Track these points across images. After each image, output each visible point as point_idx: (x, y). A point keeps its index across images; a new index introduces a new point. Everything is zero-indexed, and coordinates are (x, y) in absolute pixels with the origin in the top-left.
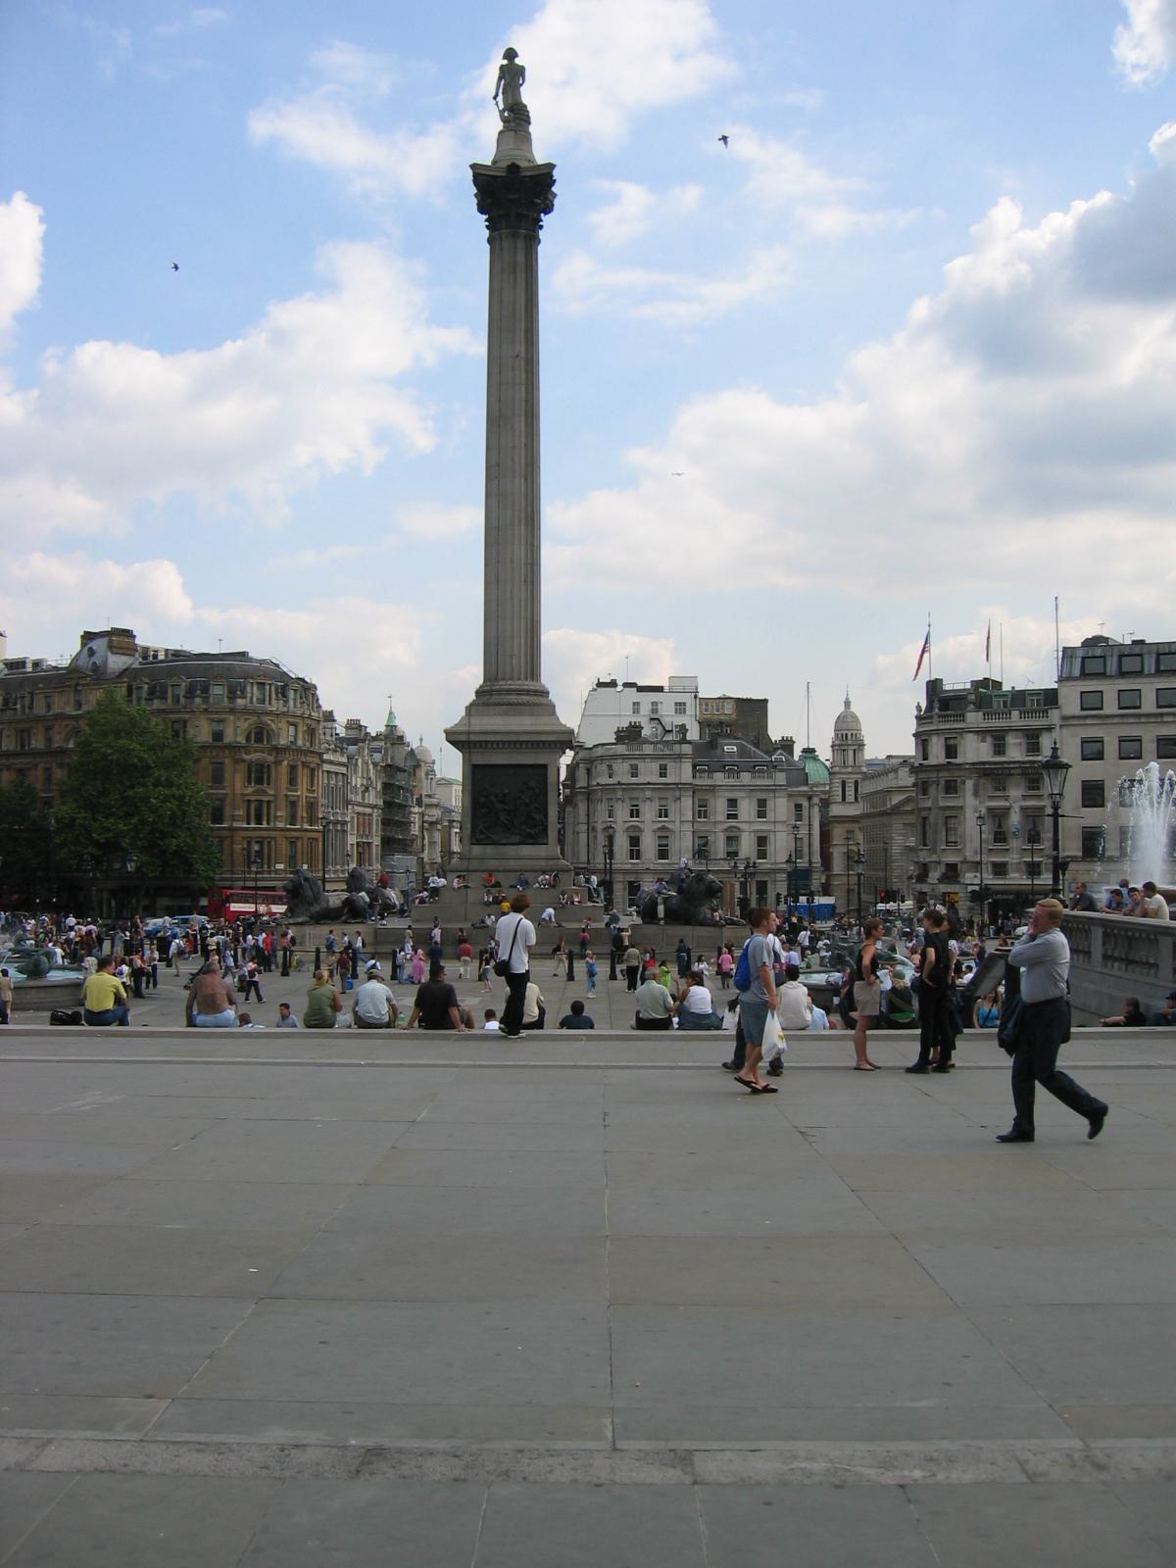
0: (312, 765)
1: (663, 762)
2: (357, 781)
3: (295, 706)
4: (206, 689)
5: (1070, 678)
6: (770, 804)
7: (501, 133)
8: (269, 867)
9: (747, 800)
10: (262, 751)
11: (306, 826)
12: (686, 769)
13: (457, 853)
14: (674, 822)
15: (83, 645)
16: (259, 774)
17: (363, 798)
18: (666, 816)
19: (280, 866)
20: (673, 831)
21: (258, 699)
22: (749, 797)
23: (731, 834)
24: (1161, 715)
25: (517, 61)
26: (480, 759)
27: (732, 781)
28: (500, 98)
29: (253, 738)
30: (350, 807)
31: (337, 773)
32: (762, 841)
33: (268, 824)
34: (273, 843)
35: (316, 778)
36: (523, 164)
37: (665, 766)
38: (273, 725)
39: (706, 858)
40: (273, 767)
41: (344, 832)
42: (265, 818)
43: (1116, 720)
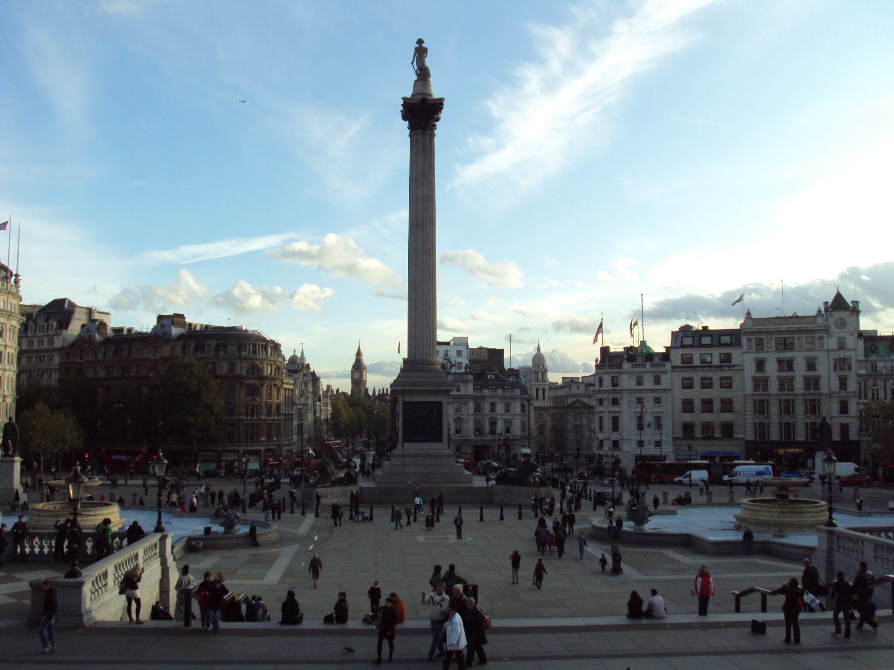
0: (279, 386)
3: (271, 355)
4: (225, 347)
5: (675, 348)
6: (512, 405)
7: (416, 82)
8: (257, 439)
9: (500, 404)
11: (276, 417)
15: (158, 322)
16: (254, 391)
19: (263, 439)
20: (463, 420)
24: (722, 367)
25: (424, 45)
26: (408, 399)
27: (492, 394)
28: (415, 63)
32: (508, 423)
33: (257, 417)
34: (260, 427)
36: (427, 97)
39: (482, 434)
40: (260, 388)
41: (292, 419)
42: (256, 414)
43: (699, 369)
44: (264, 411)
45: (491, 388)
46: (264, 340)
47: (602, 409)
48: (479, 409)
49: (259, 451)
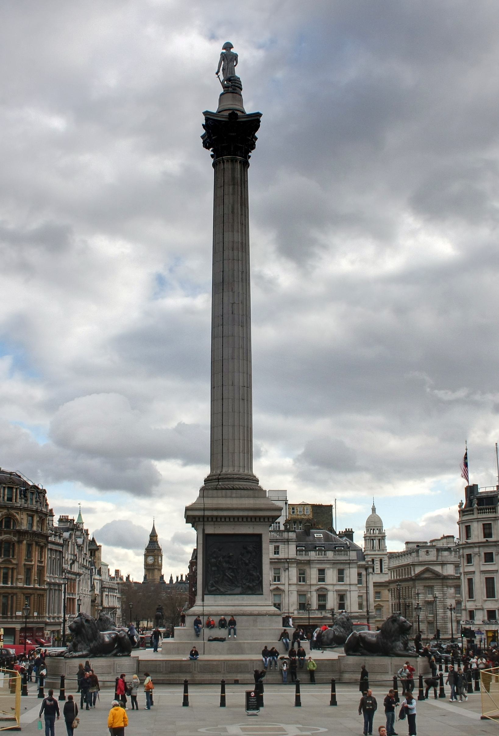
0: (42, 544)
1: (277, 544)
2: (68, 556)
6: (346, 572)
8: (12, 614)
9: (331, 570)
10: (9, 533)
11: (37, 586)
12: (292, 548)
13: (106, 608)
14: (284, 584)
17: (71, 568)
18: (279, 580)
19: (19, 614)
20: (284, 591)
21: (7, 498)
22: (332, 568)
23: (321, 593)
27: (321, 557)
29: (4, 524)
30: (64, 574)
31: (56, 551)
33: (12, 584)
34: (15, 597)
35: (44, 554)
37: (278, 547)
38: (17, 516)
40: (16, 546)
42: (10, 580)
44: (21, 576)
45: (319, 550)
46: (25, 483)
47: (471, 569)
48: (304, 578)
49: (14, 629)
